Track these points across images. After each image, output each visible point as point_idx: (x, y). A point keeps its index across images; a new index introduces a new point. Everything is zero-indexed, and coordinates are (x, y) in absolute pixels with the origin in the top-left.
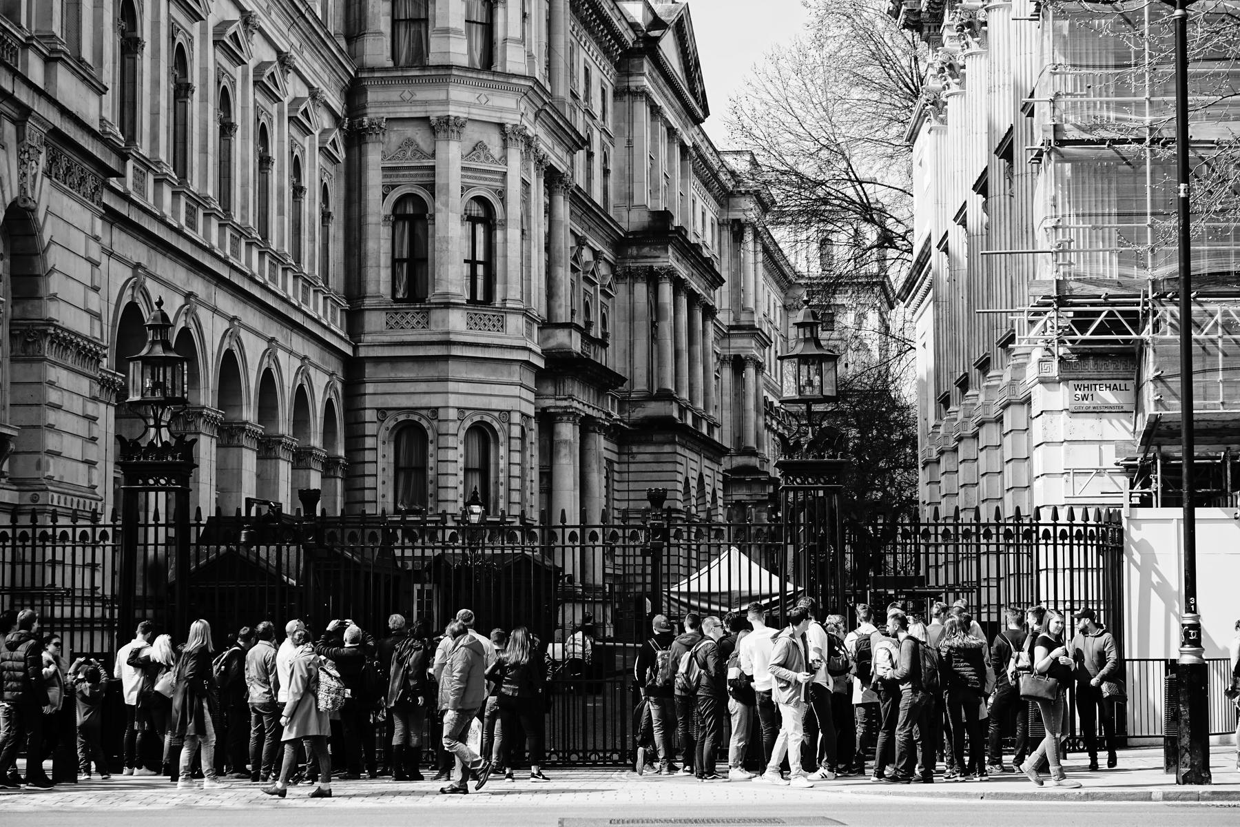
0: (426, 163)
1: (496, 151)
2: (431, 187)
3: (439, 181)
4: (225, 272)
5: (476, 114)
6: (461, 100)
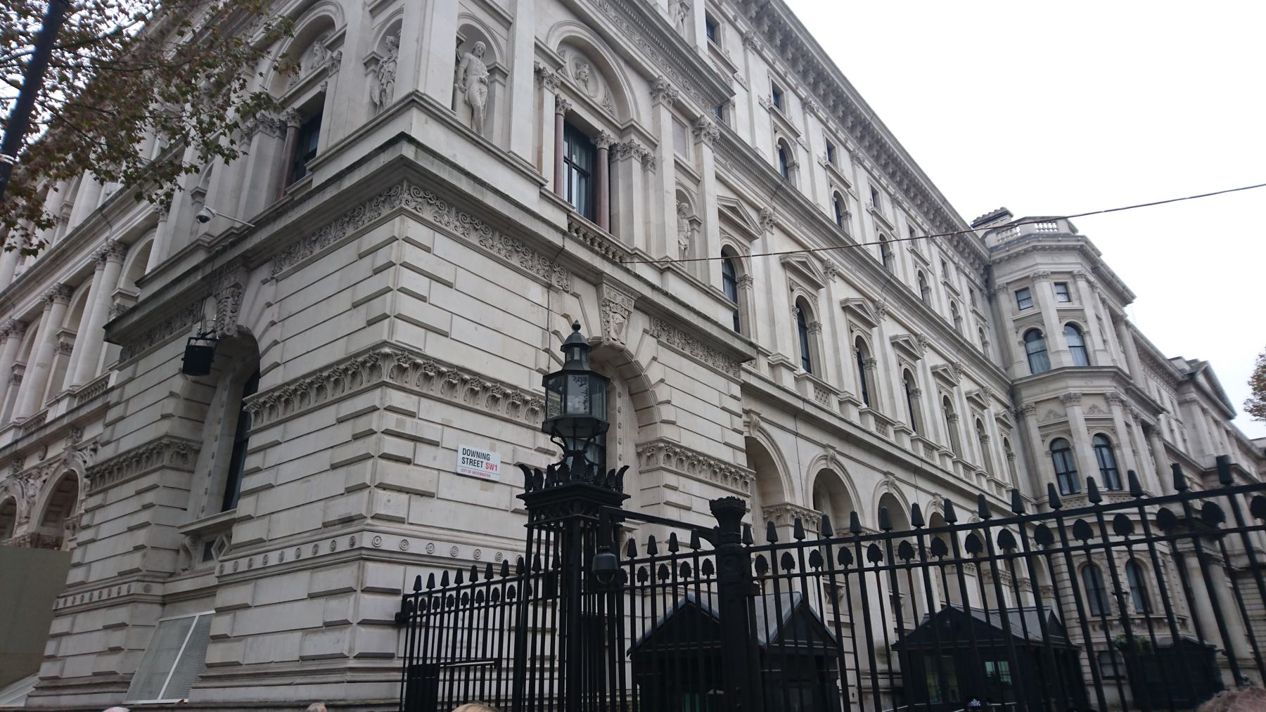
2: (1069, 432)
3: (1072, 428)
4: (918, 463)
5: (1086, 391)
6: (1075, 386)
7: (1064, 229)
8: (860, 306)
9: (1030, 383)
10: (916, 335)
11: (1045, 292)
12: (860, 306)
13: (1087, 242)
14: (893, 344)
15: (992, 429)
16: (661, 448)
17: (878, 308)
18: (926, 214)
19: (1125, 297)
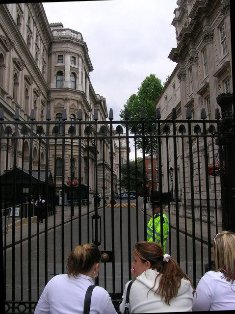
0: (63, 106)
1: (76, 105)
5: (73, 98)
6: (69, 95)
7: (79, 38)
8: (5, 41)
9: (55, 91)
10: (22, 60)
11: (68, 58)
12: (5, 41)
13: (86, 45)
14: (13, 61)
15: (39, 105)
17: (11, 44)
18: (36, 13)
19: (90, 69)
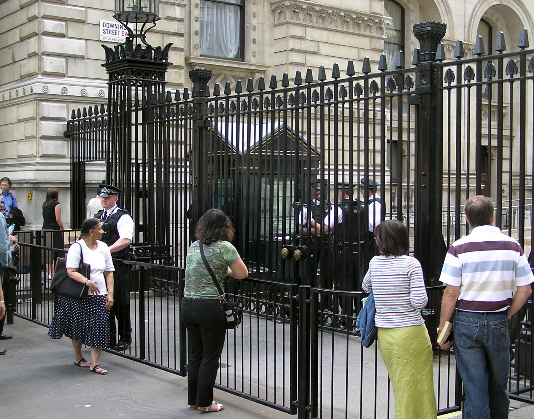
16: (287, 6)
